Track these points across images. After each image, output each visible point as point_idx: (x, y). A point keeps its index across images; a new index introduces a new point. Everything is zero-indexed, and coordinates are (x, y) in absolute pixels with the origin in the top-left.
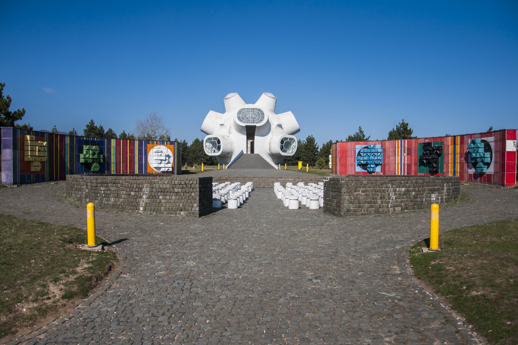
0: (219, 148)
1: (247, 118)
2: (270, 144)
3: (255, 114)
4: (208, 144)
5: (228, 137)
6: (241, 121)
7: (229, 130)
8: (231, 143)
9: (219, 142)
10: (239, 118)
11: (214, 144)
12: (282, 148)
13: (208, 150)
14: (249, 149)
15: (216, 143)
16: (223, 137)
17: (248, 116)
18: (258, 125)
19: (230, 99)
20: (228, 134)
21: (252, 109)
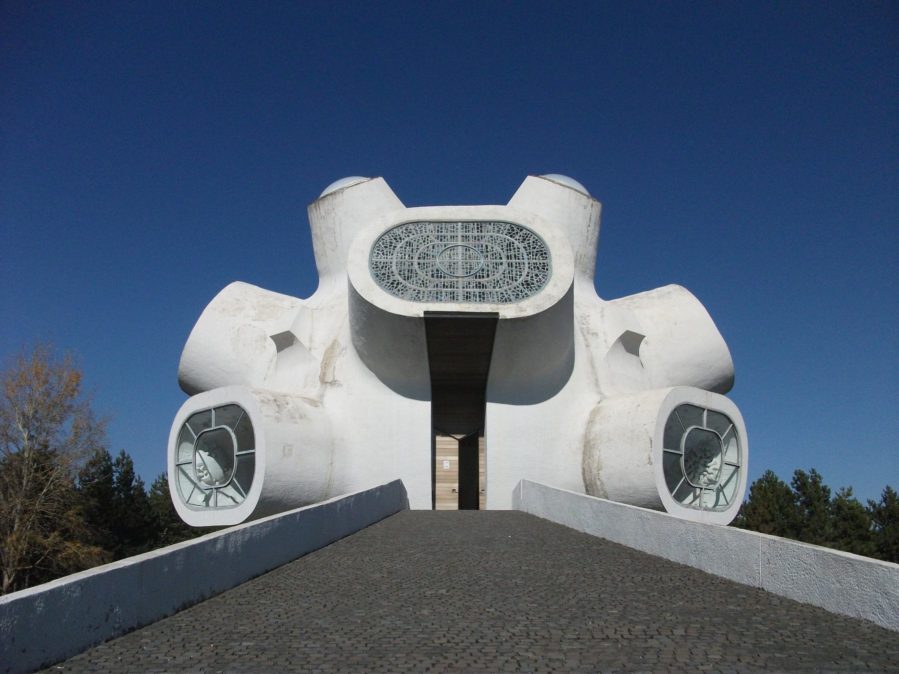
0: (243, 473)
1: (437, 274)
2: (588, 446)
3: (485, 251)
4: (187, 452)
5: (314, 403)
6: (394, 287)
7: (326, 364)
8: (332, 446)
9: (247, 437)
10: (382, 274)
11: (218, 447)
12: (671, 474)
13: (187, 487)
14: (450, 487)
15: (229, 440)
16: (278, 402)
17: (440, 262)
18: (508, 311)
19: (339, 198)
20: (313, 392)
21: (466, 224)
